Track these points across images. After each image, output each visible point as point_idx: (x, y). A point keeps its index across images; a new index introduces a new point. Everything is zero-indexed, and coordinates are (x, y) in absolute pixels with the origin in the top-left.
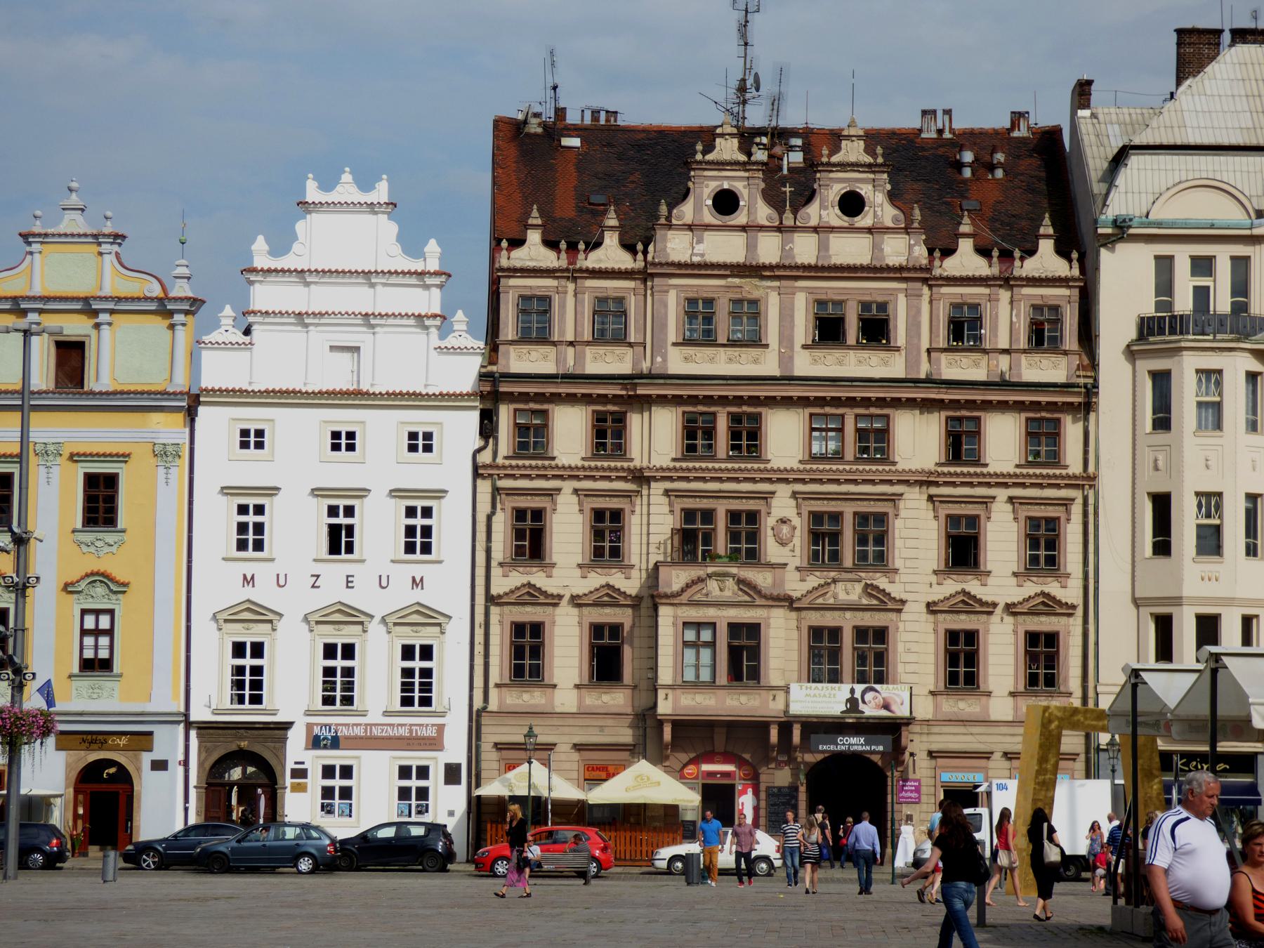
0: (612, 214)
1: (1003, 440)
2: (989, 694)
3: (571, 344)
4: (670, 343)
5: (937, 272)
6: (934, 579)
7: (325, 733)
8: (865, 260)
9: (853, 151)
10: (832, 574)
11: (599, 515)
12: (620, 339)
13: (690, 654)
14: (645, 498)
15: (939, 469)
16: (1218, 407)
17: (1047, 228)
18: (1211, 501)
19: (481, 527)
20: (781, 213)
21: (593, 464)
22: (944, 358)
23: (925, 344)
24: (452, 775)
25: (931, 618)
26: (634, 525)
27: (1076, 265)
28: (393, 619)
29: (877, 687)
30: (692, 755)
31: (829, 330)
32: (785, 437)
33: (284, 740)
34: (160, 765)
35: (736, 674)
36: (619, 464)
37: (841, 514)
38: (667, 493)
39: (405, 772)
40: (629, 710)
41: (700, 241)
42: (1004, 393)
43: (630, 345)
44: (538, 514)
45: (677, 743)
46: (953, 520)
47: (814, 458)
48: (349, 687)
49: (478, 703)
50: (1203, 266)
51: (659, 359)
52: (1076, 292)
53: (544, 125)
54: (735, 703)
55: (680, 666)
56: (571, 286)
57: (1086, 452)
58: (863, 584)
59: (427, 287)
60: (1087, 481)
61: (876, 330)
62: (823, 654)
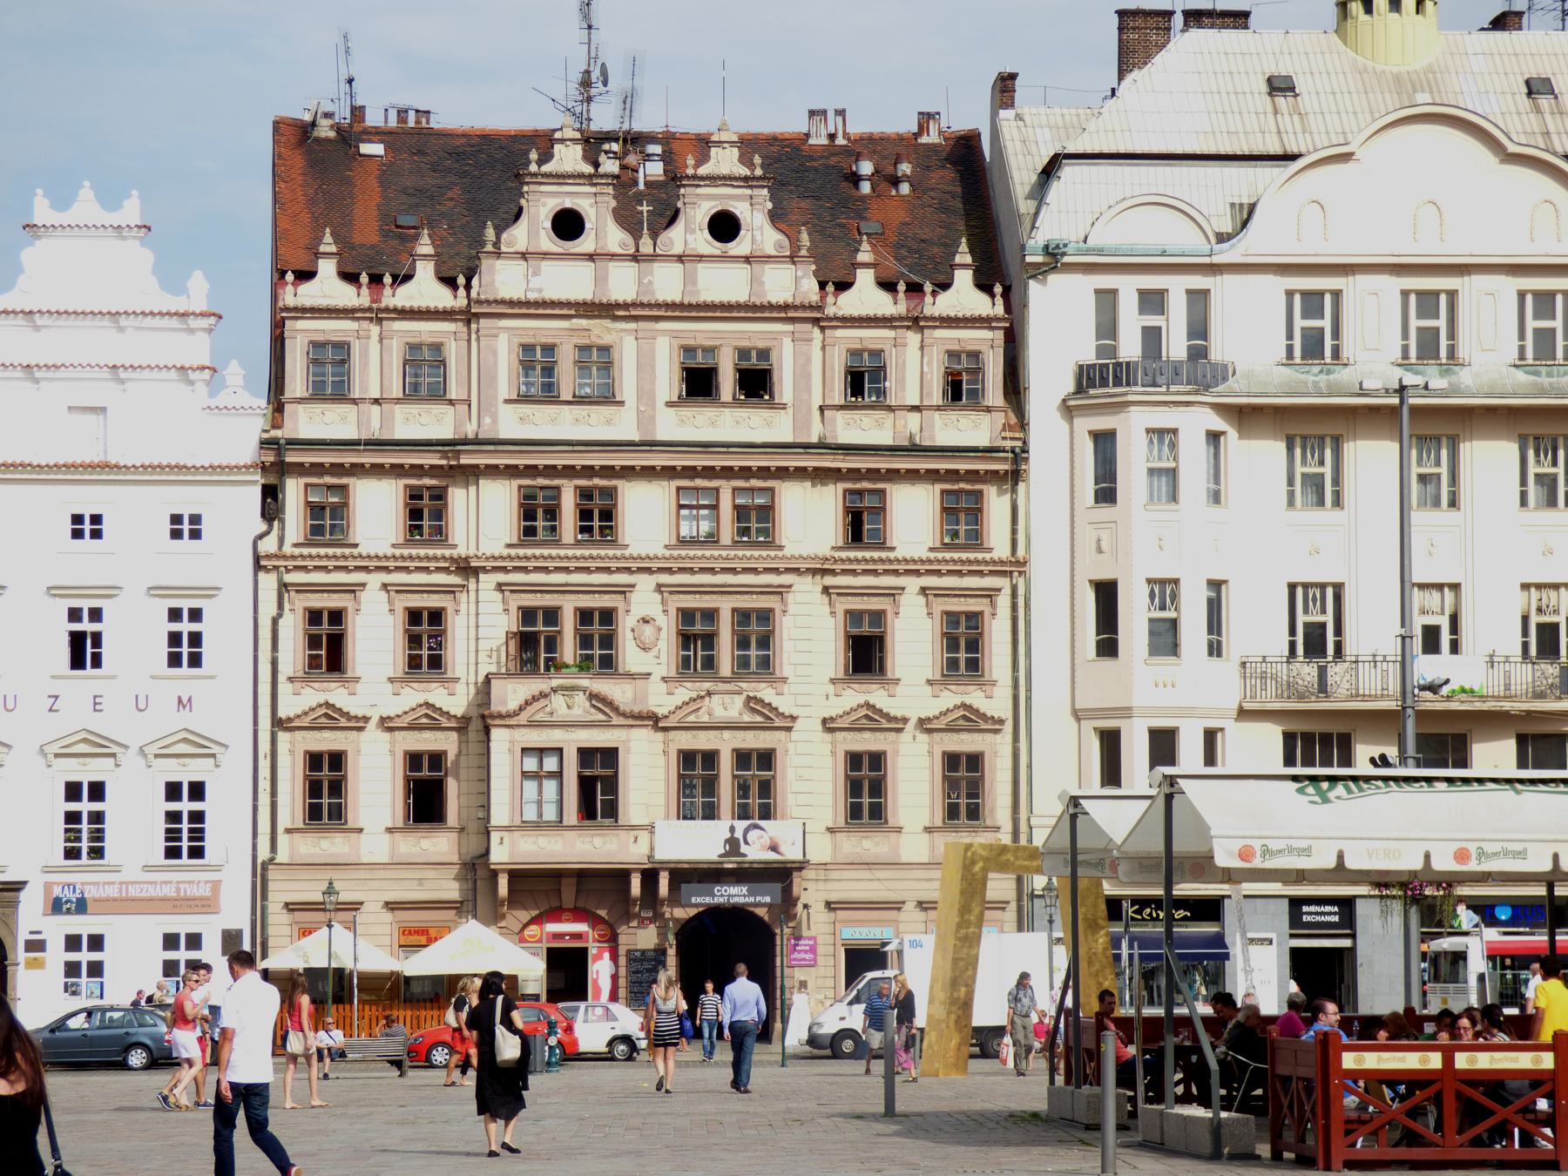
0: (425, 239)
1: (913, 516)
2: (899, 830)
3: (376, 401)
4: (501, 400)
5: (830, 311)
6: (831, 689)
7: (68, 894)
8: (741, 296)
9: (725, 161)
10: (707, 685)
11: (414, 616)
12: (438, 394)
13: (531, 787)
14: (472, 595)
15: (837, 554)
16: (1173, 473)
17: (964, 256)
18: (1165, 590)
20: (637, 238)
21: (406, 552)
22: (840, 416)
23: (817, 401)
25: (828, 737)
26: (458, 629)
27: (999, 301)
28: (153, 749)
29: (762, 823)
30: (535, 913)
31: (699, 383)
32: (646, 514)
33: (14, 904)
35: (588, 811)
36: (439, 552)
37: (716, 610)
38: (500, 587)
39: (171, 941)
40: (455, 859)
41: (536, 274)
42: (915, 460)
43: (451, 402)
44: (337, 616)
45: (515, 899)
46: (854, 616)
47: (683, 542)
48: (98, 836)
49: (264, 853)
50: (1153, 301)
51: (487, 420)
52: (1000, 334)
53: (338, 128)
54: (588, 847)
55: (519, 801)
56: (375, 330)
57: (1014, 532)
58: (744, 696)
59: (192, 331)
60: (1015, 566)
61: (756, 383)
62: (696, 778)
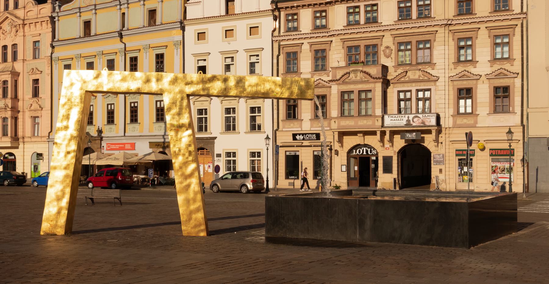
10: (408, 68)
15: (454, 19)
19: (275, 61)
33: (214, 143)
49: (275, 128)
54: (362, 124)
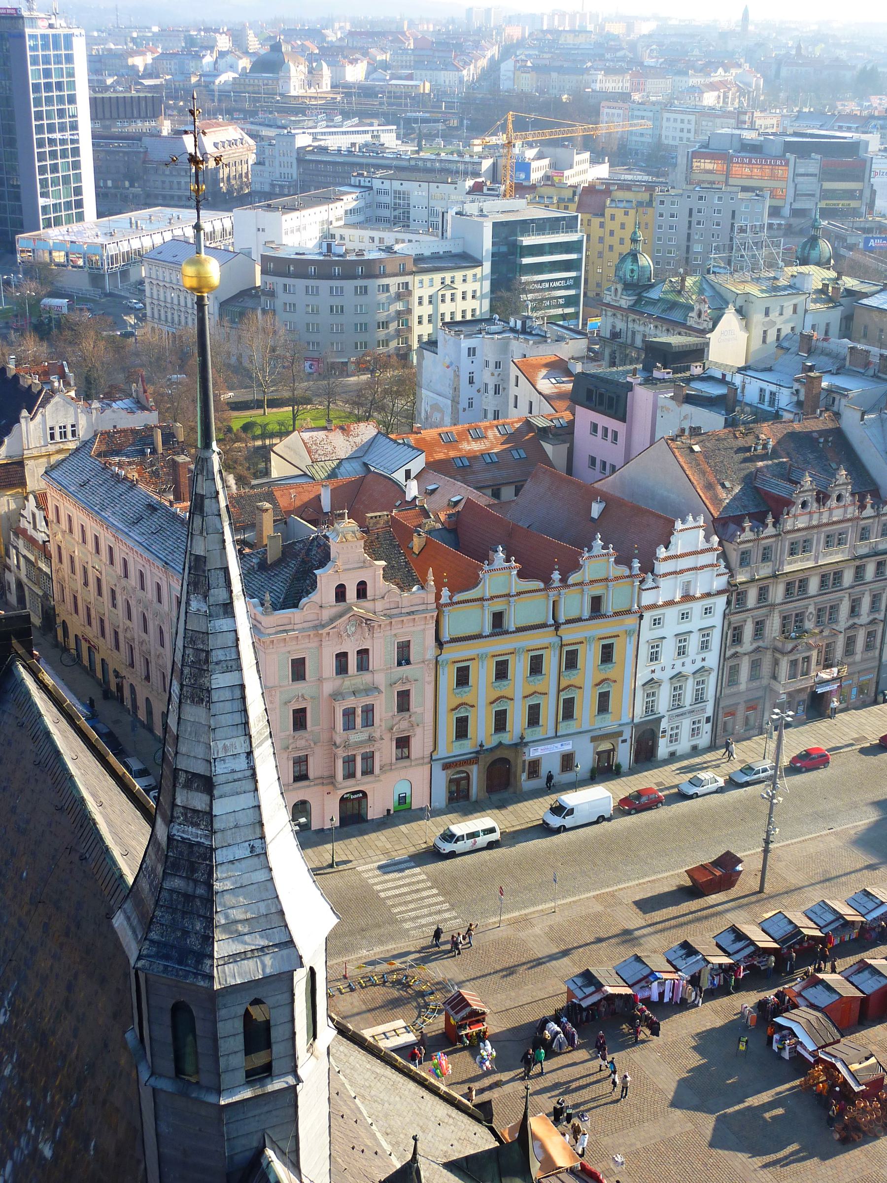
24: (708, 720)
26: (768, 623)
32: (813, 586)
34: (624, 741)
